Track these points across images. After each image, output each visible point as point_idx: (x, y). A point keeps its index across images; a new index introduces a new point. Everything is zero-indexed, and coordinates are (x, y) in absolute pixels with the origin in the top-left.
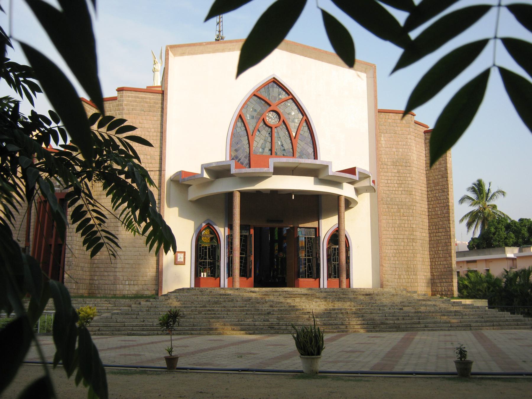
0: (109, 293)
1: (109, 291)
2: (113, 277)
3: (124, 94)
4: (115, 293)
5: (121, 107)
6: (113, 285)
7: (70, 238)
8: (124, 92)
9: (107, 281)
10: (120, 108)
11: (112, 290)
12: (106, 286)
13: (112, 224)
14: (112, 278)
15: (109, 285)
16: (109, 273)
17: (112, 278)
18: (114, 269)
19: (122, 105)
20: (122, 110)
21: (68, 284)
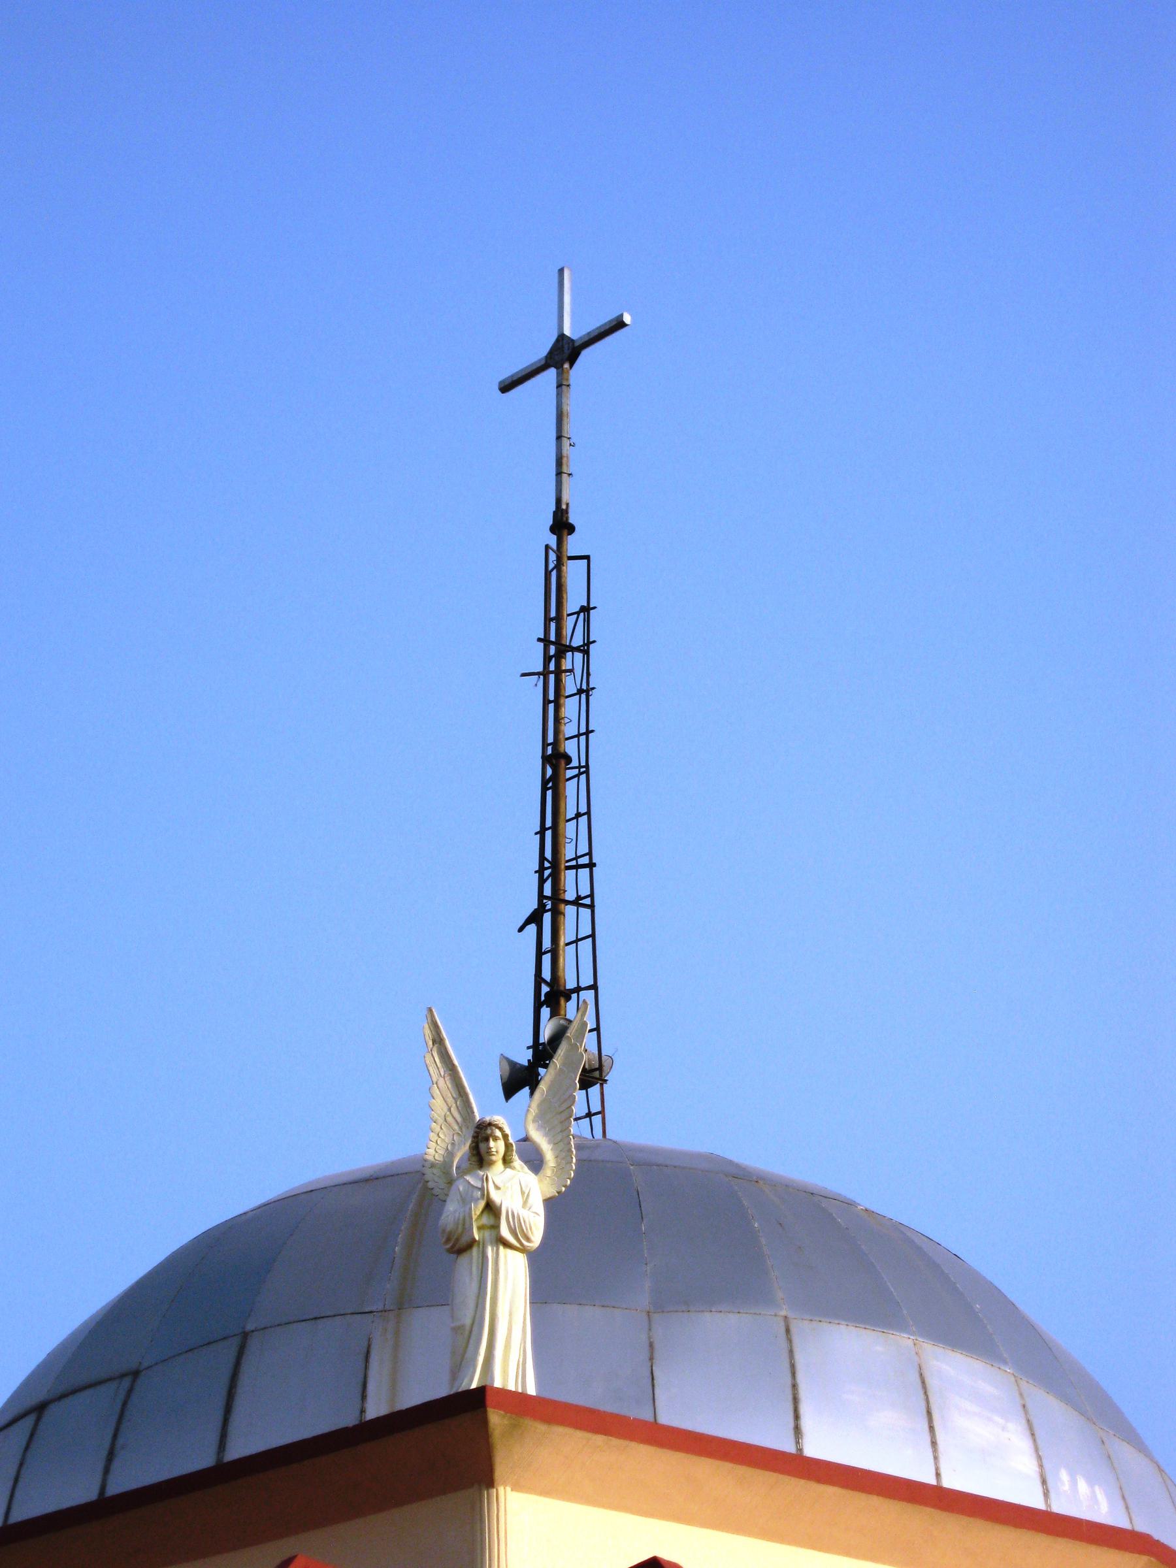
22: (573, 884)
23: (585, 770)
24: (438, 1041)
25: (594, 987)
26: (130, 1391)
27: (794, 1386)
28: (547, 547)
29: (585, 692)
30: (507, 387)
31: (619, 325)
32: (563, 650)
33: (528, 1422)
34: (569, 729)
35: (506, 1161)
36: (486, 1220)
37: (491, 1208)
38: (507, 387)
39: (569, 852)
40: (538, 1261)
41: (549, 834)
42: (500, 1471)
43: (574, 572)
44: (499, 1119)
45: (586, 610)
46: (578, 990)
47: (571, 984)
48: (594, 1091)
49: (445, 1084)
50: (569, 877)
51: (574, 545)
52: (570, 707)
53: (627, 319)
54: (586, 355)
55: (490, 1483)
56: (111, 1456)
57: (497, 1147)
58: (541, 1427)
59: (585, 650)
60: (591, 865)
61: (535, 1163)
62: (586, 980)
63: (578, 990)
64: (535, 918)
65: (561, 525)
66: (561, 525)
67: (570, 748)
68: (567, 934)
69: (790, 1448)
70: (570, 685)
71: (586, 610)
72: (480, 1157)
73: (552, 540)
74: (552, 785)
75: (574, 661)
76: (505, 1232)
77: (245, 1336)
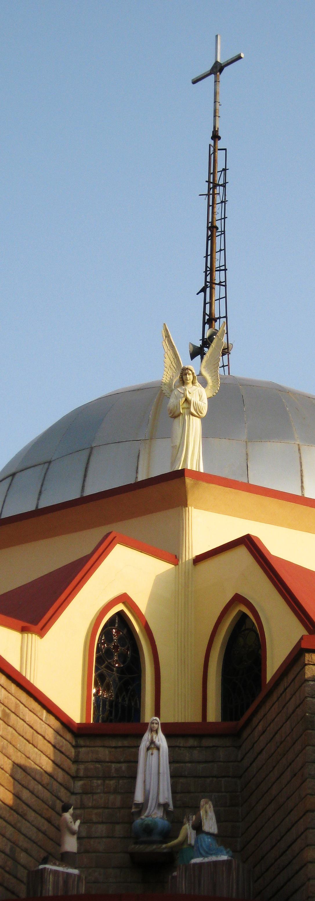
22: (218, 277)
23: (223, 232)
24: (167, 336)
25: (226, 317)
26: (48, 469)
27: (301, 471)
28: (210, 145)
29: (224, 202)
30: (195, 82)
31: (239, 58)
32: (215, 185)
33: (200, 482)
34: (218, 217)
35: (193, 383)
36: (185, 405)
37: (187, 401)
38: (195, 82)
39: (217, 264)
40: (205, 421)
41: (209, 257)
42: (189, 502)
43: (220, 155)
44: (191, 367)
45: (225, 170)
46: (219, 318)
47: (217, 316)
48: (225, 357)
49: (170, 353)
50: (217, 274)
51: (220, 144)
52: (218, 208)
53: (242, 55)
54: (226, 69)
55: (186, 505)
56: (40, 493)
57: (190, 377)
58: (205, 484)
59: (224, 185)
60: (225, 270)
61: (204, 384)
62: (223, 314)
63: (219, 318)
64: (203, 290)
65: (216, 137)
66: (216, 137)
67: (218, 224)
68: (216, 296)
69: (299, 494)
70: (218, 199)
71: (225, 170)
72: (183, 381)
73: (212, 142)
74: (211, 238)
75: (219, 190)
77: (92, 448)
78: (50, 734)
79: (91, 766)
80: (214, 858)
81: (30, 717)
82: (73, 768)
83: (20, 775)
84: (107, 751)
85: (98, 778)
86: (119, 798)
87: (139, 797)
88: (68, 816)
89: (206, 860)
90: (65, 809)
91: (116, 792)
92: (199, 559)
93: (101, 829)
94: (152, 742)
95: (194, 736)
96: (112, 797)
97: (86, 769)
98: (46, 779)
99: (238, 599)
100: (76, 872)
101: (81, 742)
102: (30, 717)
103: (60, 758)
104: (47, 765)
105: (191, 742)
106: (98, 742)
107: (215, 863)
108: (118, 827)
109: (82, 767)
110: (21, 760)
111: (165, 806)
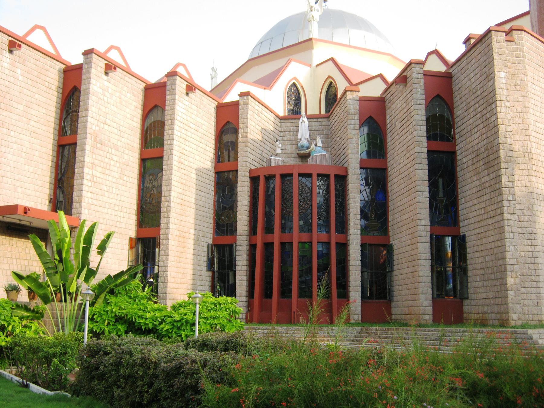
0: (531, 318)
1: (531, 316)
2: (534, 295)
3: (523, 36)
4: (540, 319)
5: (521, 53)
6: (536, 308)
7: (511, 234)
8: (523, 32)
9: (526, 301)
10: (520, 54)
11: (535, 314)
12: (526, 308)
13: (526, 218)
14: (533, 296)
15: (530, 307)
16: (529, 289)
17: (533, 296)
18: (535, 283)
19: (521, 50)
20: (523, 58)
21: (516, 305)
40: (318, 22)
42: (314, 47)
57: (313, 9)
69: (348, 44)
72: (311, 10)
76: (314, 19)
78: (272, 119)
79: (285, 128)
80: (321, 154)
81: (266, 114)
82: (280, 129)
83: (263, 131)
84: (290, 123)
85: (287, 132)
86: (294, 137)
87: (299, 137)
88: (277, 143)
89: (319, 154)
90: (277, 141)
91: (293, 136)
92: (317, 66)
93: (289, 147)
94: (303, 120)
95: (315, 118)
96: (292, 137)
97: (284, 129)
98: (272, 133)
99: (329, 77)
100: (281, 159)
101: (282, 121)
102: (266, 114)
103: (276, 126)
104: (272, 129)
105: (315, 120)
106: (287, 121)
107: (321, 155)
108: (294, 146)
109: (282, 128)
110: (264, 127)
111: (307, 139)
